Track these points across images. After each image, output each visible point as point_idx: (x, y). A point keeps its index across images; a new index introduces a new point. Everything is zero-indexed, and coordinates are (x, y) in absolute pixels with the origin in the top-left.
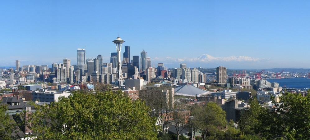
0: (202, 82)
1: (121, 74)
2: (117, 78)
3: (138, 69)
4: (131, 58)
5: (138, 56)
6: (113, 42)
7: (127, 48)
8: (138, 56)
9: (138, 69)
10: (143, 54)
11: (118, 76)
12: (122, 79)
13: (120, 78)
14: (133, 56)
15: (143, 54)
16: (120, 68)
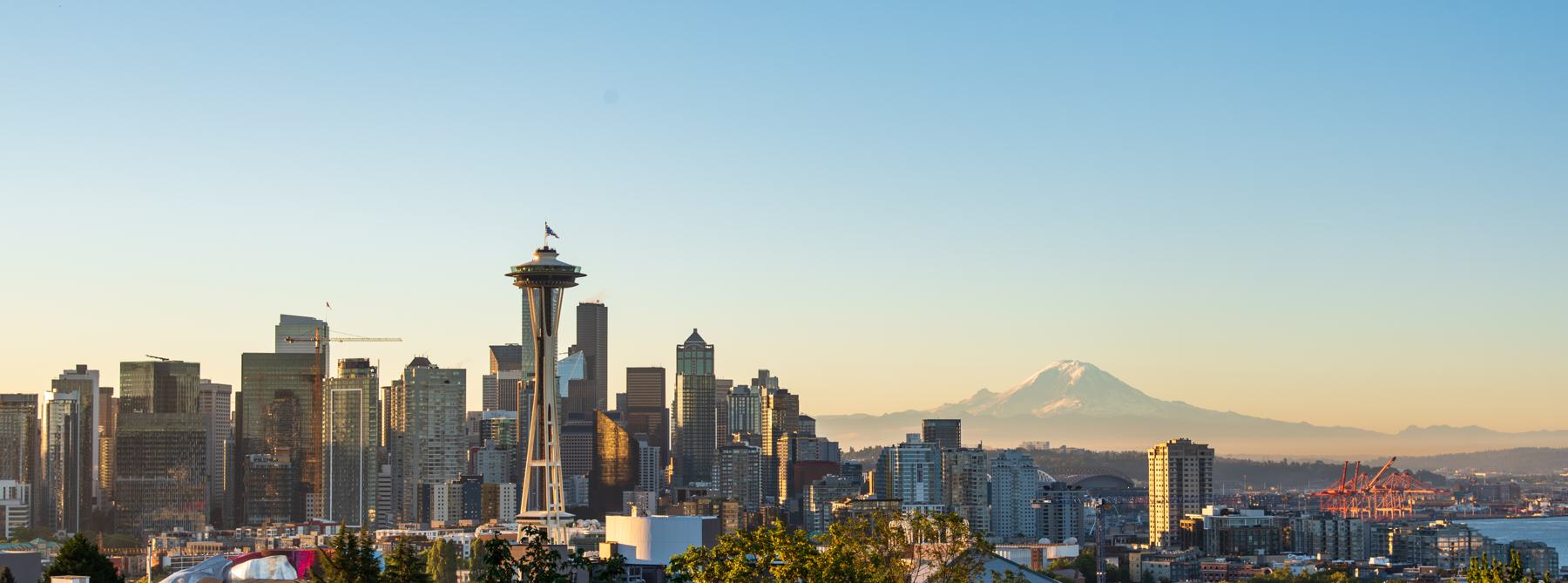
0: (1058, 540)
1: (555, 483)
2: (531, 507)
3: (657, 449)
4: (616, 384)
5: (661, 371)
6: (513, 279)
7: (593, 318)
8: (661, 372)
9: (657, 449)
10: (695, 352)
11: (538, 502)
12: (563, 513)
13: (548, 505)
14: (629, 370)
15: (695, 352)
16: (554, 443)
